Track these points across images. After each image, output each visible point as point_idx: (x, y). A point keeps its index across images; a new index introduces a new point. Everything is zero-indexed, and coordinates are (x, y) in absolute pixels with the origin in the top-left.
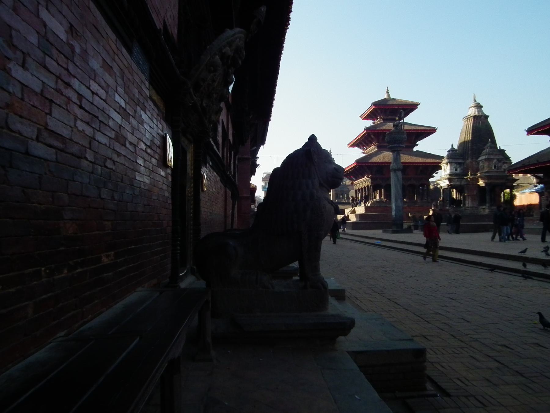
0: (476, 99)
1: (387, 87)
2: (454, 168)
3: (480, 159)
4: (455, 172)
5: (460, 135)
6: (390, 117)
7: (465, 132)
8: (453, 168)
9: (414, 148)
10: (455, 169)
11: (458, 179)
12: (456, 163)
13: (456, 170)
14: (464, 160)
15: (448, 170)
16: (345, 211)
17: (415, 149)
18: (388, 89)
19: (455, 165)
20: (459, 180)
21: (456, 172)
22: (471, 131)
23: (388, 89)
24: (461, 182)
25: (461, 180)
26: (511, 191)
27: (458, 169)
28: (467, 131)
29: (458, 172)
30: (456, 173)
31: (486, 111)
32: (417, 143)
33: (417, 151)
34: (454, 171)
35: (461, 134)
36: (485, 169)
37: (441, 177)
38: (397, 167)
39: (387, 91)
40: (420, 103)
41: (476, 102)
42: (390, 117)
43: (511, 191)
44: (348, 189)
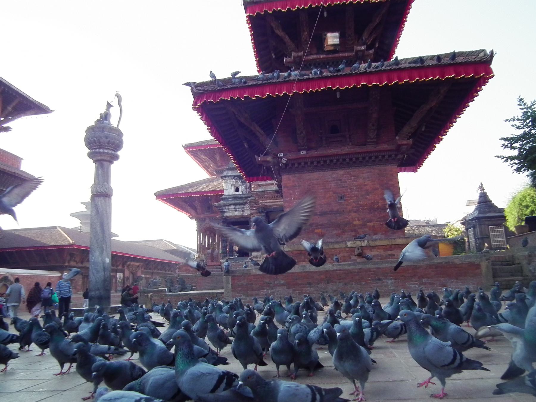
2: (232, 186)
8: (230, 187)
11: (235, 204)
13: (237, 190)
19: (234, 180)
20: (237, 207)
25: (242, 206)
29: (240, 192)
38: (95, 190)
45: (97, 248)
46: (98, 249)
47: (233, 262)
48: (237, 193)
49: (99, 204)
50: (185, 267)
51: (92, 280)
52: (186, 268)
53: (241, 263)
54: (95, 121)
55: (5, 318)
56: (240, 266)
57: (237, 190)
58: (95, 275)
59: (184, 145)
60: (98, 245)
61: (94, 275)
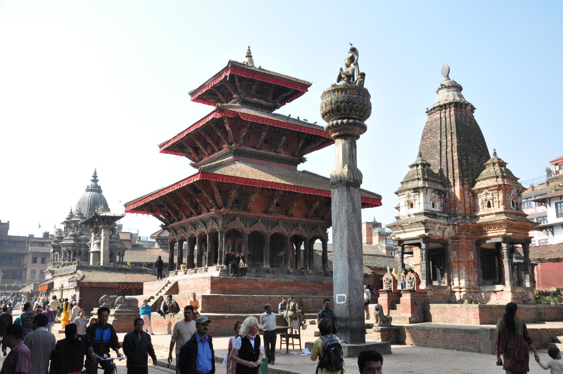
0: (449, 75)
1: (249, 47)
2: (431, 200)
3: (478, 185)
4: (433, 209)
5: (423, 139)
7: (439, 131)
9: (299, 165)
12: (435, 190)
14: (445, 187)
15: (420, 203)
16: (144, 286)
17: (301, 167)
21: (434, 209)
22: (454, 130)
23: (249, 50)
24: (443, 232)
28: (444, 130)
30: (433, 211)
32: (305, 156)
33: (304, 172)
34: (430, 207)
35: (425, 137)
36: (496, 204)
37: (398, 218)
39: (247, 54)
40: (311, 84)
41: (449, 79)
44: (124, 245)
45: (356, 259)
46: (357, 260)
47: (436, 291)
49: (356, 197)
50: (220, 283)
51: (352, 305)
52: (221, 285)
53: (442, 292)
54: (473, 109)
55: (387, 356)
56: (442, 295)
58: (356, 298)
59: (548, 168)
60: (357, 256)
61: (354, 298)
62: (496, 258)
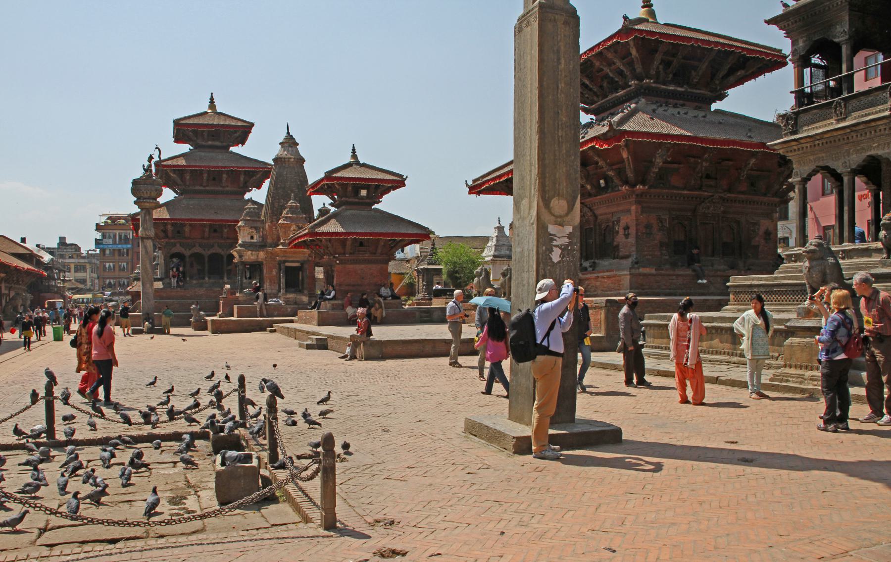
1: (212, 94)
4: (250, 241)
6: (210, 143)
8: (247, 235)
10: (249, 236)
13: (252, 238)
18: (212, 96)
21: (252, 241)
23: (212, 96)
25: (258, 252)
26: (331, 268)
27: (255, 238)
29: (255, 240)
31: (302, 150)
34: (248, 239)
42: (210, 143)
43: (331, 268)
48: (252, 241)
57: (252, 238)
62: (301, 273)
